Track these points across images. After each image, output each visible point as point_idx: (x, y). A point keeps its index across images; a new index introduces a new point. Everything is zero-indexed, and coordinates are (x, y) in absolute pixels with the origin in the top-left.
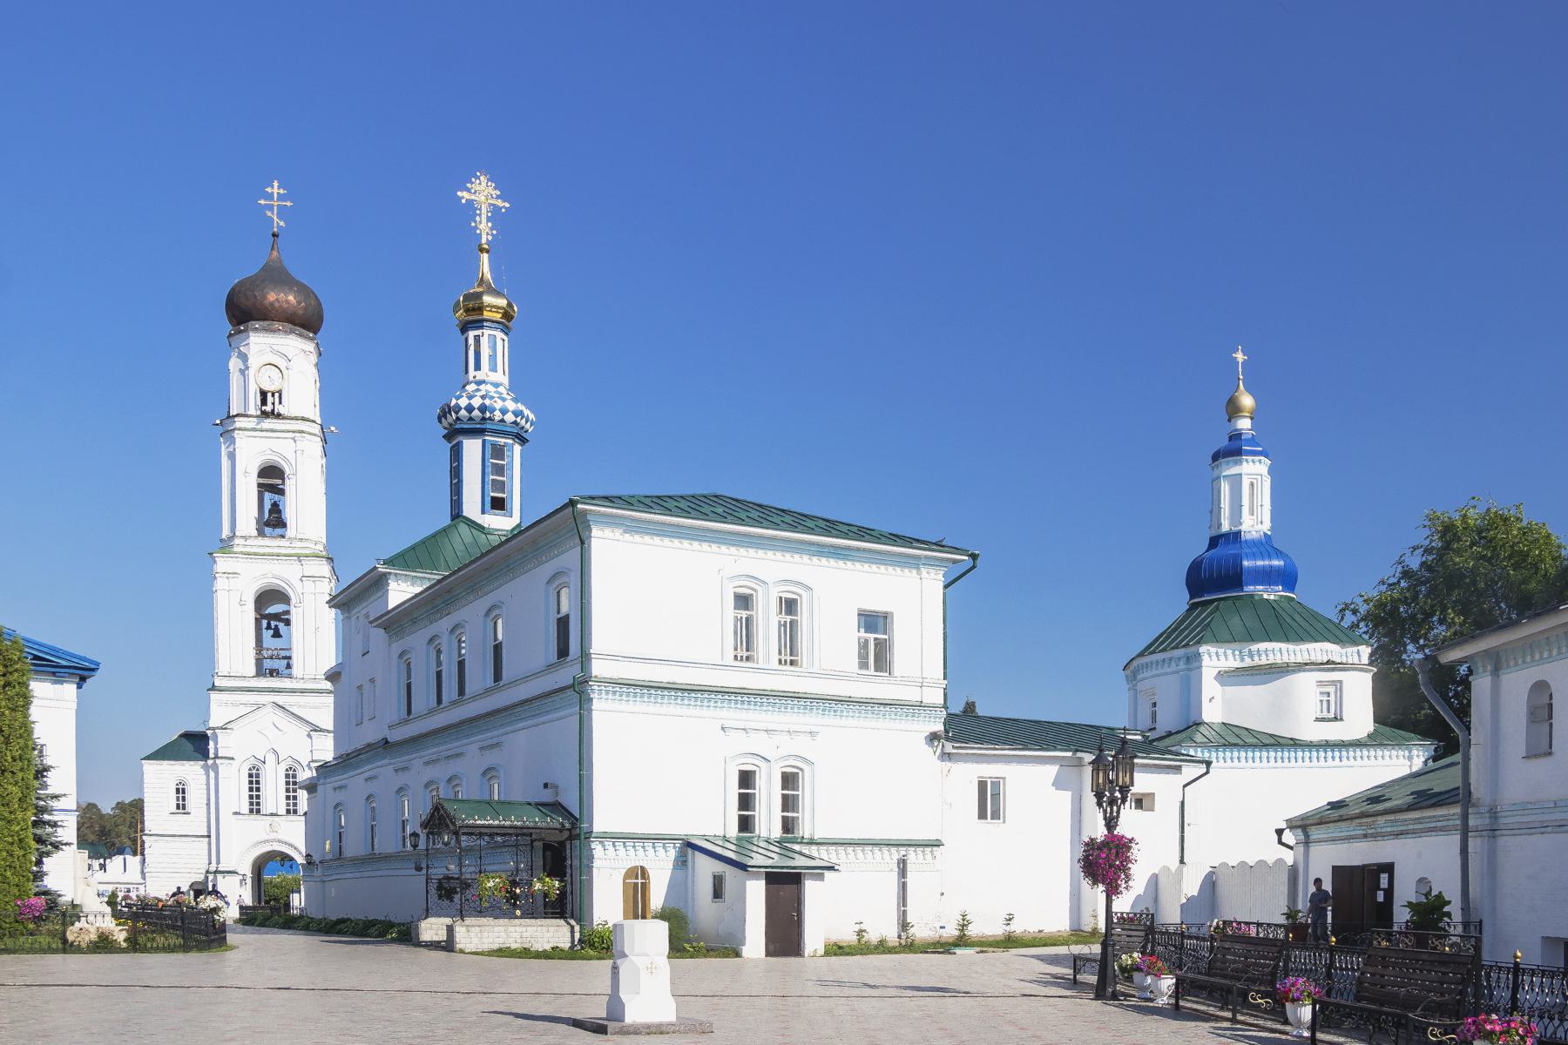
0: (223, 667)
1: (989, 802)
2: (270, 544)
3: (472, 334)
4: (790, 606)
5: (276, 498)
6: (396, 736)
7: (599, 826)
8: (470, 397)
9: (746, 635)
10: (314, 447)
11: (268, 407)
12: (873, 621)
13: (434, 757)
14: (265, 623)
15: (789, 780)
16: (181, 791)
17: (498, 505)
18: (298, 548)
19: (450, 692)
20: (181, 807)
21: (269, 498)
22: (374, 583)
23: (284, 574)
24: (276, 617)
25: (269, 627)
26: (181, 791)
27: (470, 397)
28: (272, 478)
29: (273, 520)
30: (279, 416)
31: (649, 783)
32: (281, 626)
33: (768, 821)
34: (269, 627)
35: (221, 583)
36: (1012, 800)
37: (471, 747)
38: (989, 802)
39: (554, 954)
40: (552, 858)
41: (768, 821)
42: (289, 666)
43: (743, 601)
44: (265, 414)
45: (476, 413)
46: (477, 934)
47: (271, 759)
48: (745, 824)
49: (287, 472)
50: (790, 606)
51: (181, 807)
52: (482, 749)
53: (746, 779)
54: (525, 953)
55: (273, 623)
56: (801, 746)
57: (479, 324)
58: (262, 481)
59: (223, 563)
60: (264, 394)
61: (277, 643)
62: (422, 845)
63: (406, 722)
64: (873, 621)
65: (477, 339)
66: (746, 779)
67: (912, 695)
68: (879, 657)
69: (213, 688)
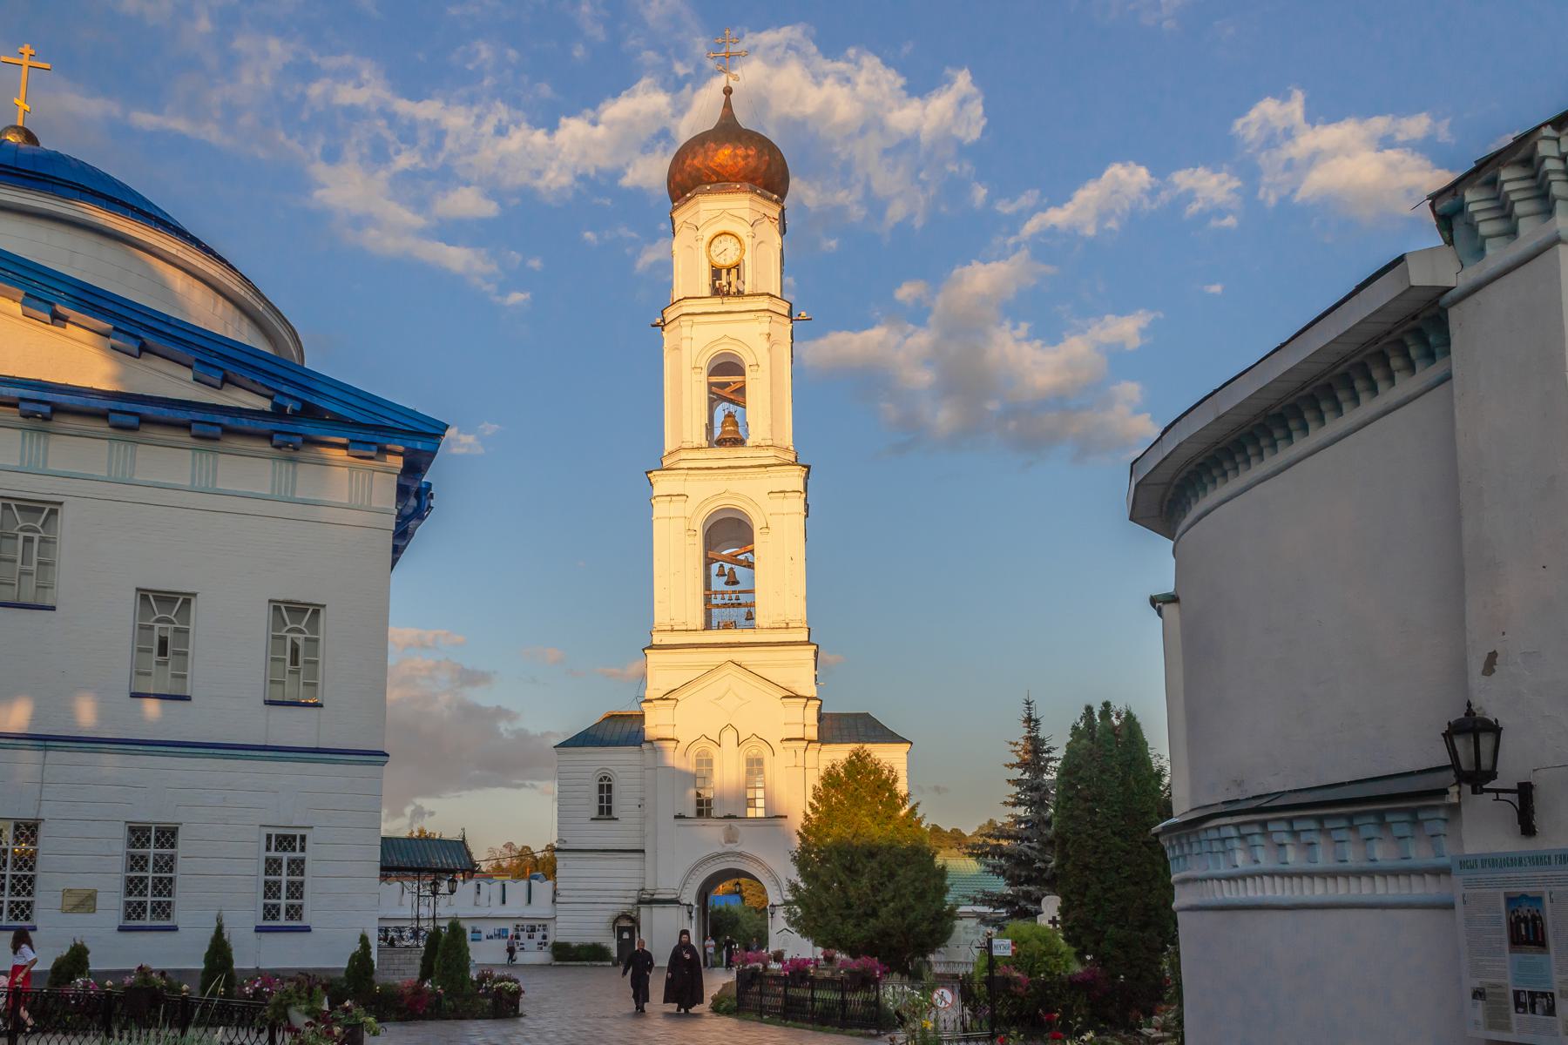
0: (661, 617)
2: (728, 455)
5: (732, 408)
16: (605, 789)
18: (768, 456)
20: (605, 811)
25: (721, 574)
26: (605, 789)
30: (740, 294)
32: (740, 572)
34: (721, 574)
35: (660, 509)
42: (750, 617)
44: (717, 292)
47: (729, 738)
49: (748, 360)
51: (605, 811)
55: (727, 567)
58: (714, 379)
59: (663, 484)
60: (716, 273)
69: (651, 647)
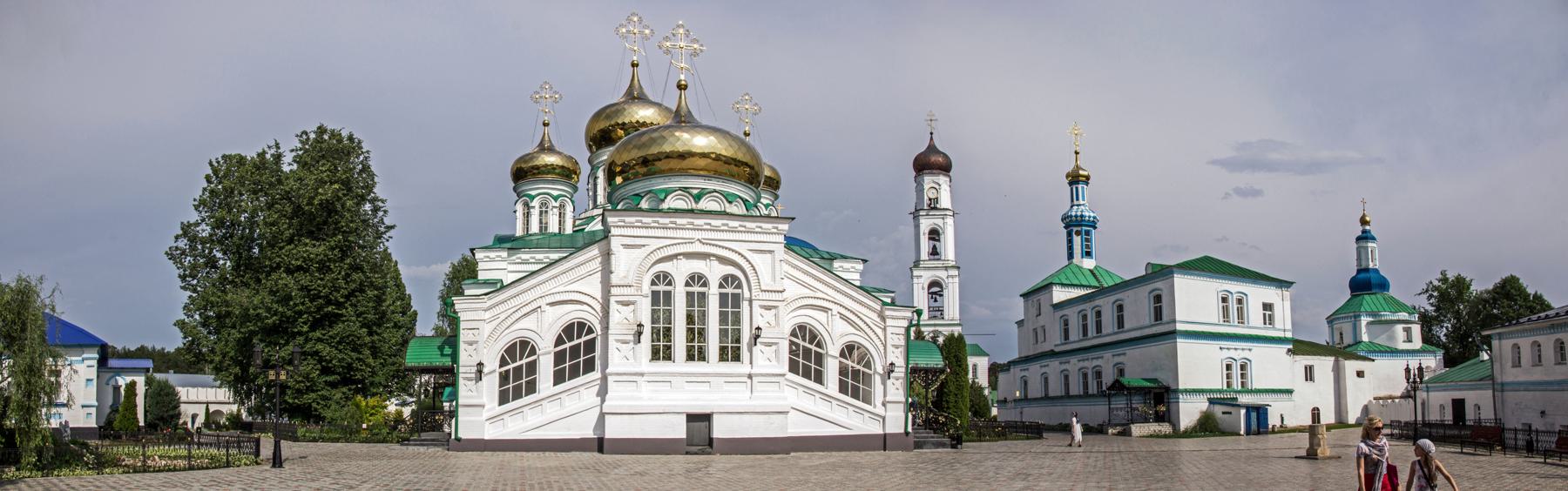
1: (1309, 373)
2: (936, 263)
4: (1240, 301)
6: (1057, 349)
7: (1181, 387)
9: (1226, 311)
10: (950, 221)
11: (933, 205)
12: (1267, 307)
15: (1243, 367)
17: (1088, 254)
19: (1092, 331)
22: (1046, 287)
23: (942, 274)
28: (935, 234)
29: (934, 252)
31: (1198, 369)
33: (1237, 385)
36: (1317, 373)
37: (1108, 354)
38: (1309, 373)
39: (1166, 436)
40: (1160, 398)
41: (1237, 385)
43: (1224, 300)
46: (1137, 430)
48: (1229, 385)
50: (1240, 301)
53: (1229, 367)
54: (1158, 436)
56: (1246, 354)
57: (1078, 182)
64: (1267, 307)
66: (1229, 367)
67: (1281, 334)
68: (1269, 320)
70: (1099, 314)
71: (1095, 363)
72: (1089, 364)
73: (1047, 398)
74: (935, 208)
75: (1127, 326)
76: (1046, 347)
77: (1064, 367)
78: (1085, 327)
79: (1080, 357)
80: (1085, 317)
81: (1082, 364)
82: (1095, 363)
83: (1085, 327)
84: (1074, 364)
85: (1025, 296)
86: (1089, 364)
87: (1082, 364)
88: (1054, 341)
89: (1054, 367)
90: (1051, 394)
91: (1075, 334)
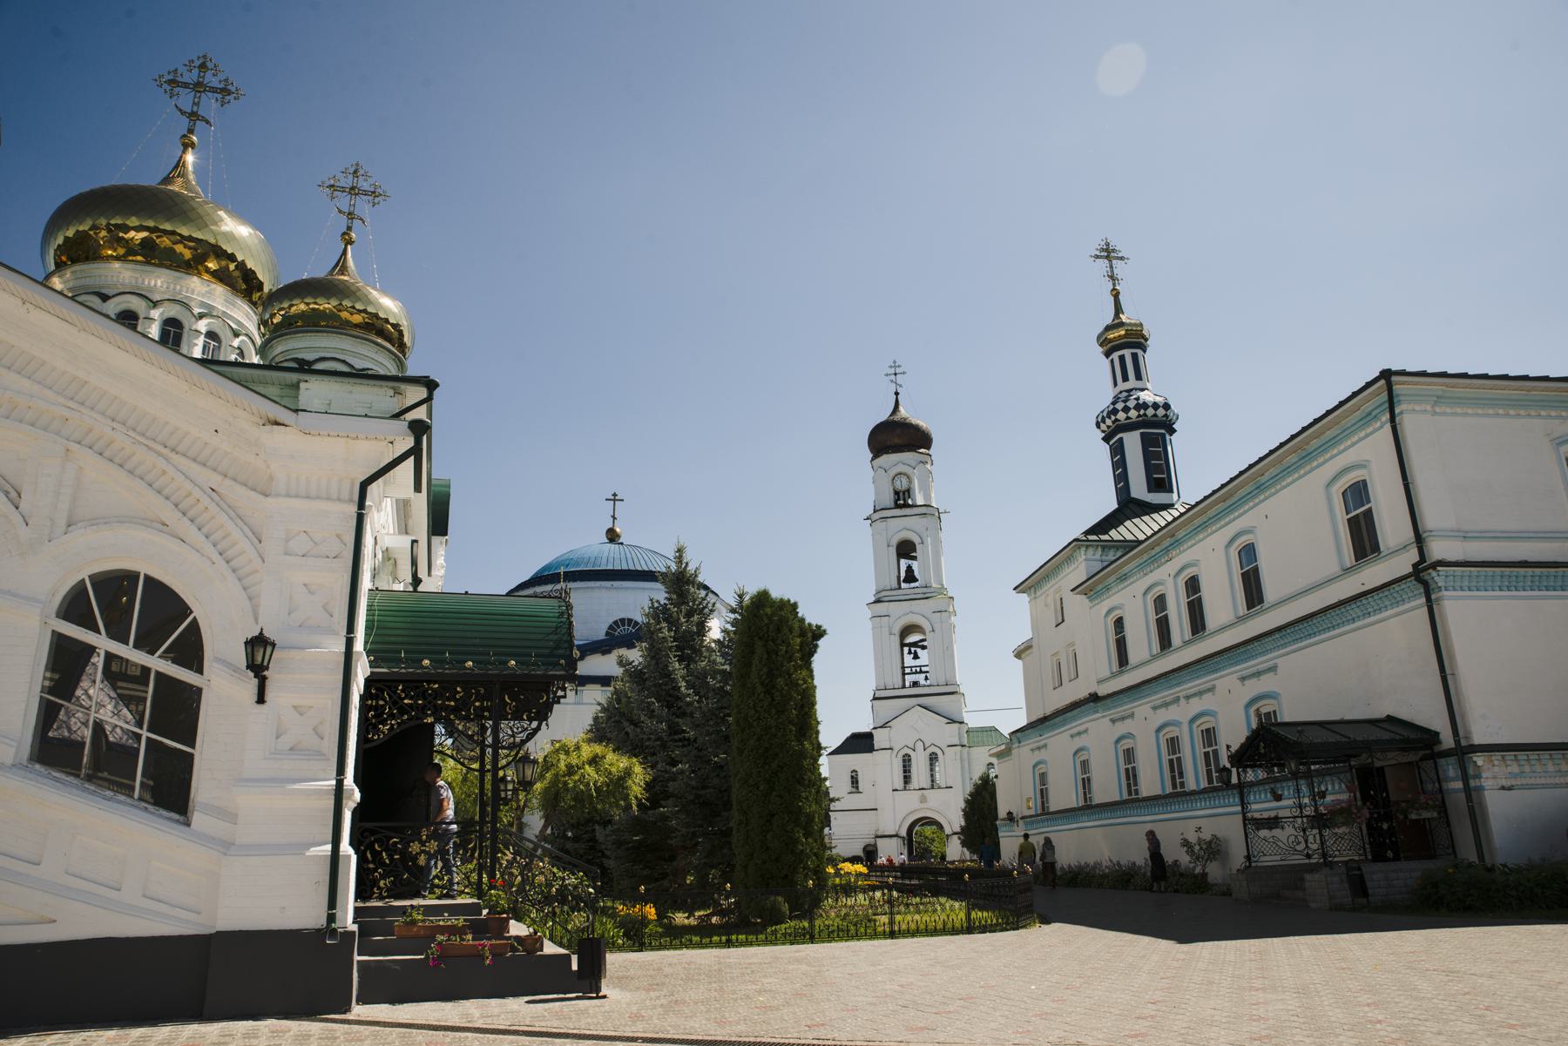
3: (1115, 356)
6: (1103, 690)
8: (1125, 401)
13: (1168, 699)
14: (906, 649)
21: (904, 563)
24: (915, 644)
27: (1125, 401)
44: (897, 506)
45: (1133, 414)
47: (920, 746)
52: (1243, 679)
61: (917, 662)
62: (1234, 780)
63: (1121, 673)
65: (1122, 358)
70: (1193, 585)
71: (1196, 706)
72: (1181, 713)
73: (1089, 808)
74: (906, 506)
75: (1270, 592)
76: (1079, 691)
77: (1122, 728)
78: (1163, 626)
79: (1157, 698)
80: (1160, 602)
81: (1164, 715)
82: (1196, 706)
83: (1163, 626)
84: (1144, 721)
85: (1027, 586)
86: (1181, 713)
87: (1164, 715)
88: (1096, 672)
89: (1098, 732)
90: (1099, 797)
91: (1141, 641)
